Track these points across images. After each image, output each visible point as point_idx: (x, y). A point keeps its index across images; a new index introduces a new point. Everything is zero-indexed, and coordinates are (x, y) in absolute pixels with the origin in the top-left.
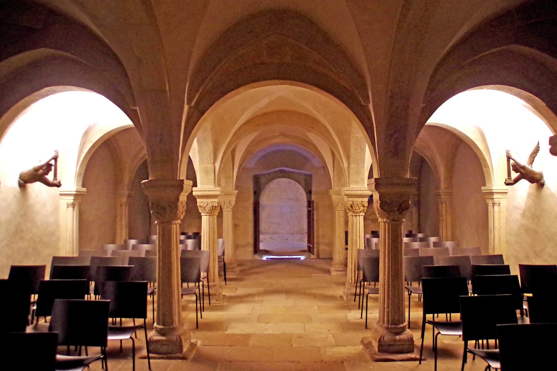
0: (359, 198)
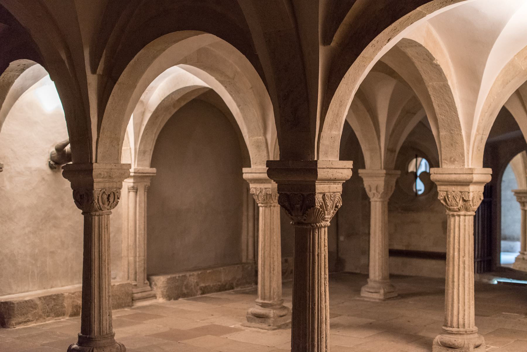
0: (456, 187)
